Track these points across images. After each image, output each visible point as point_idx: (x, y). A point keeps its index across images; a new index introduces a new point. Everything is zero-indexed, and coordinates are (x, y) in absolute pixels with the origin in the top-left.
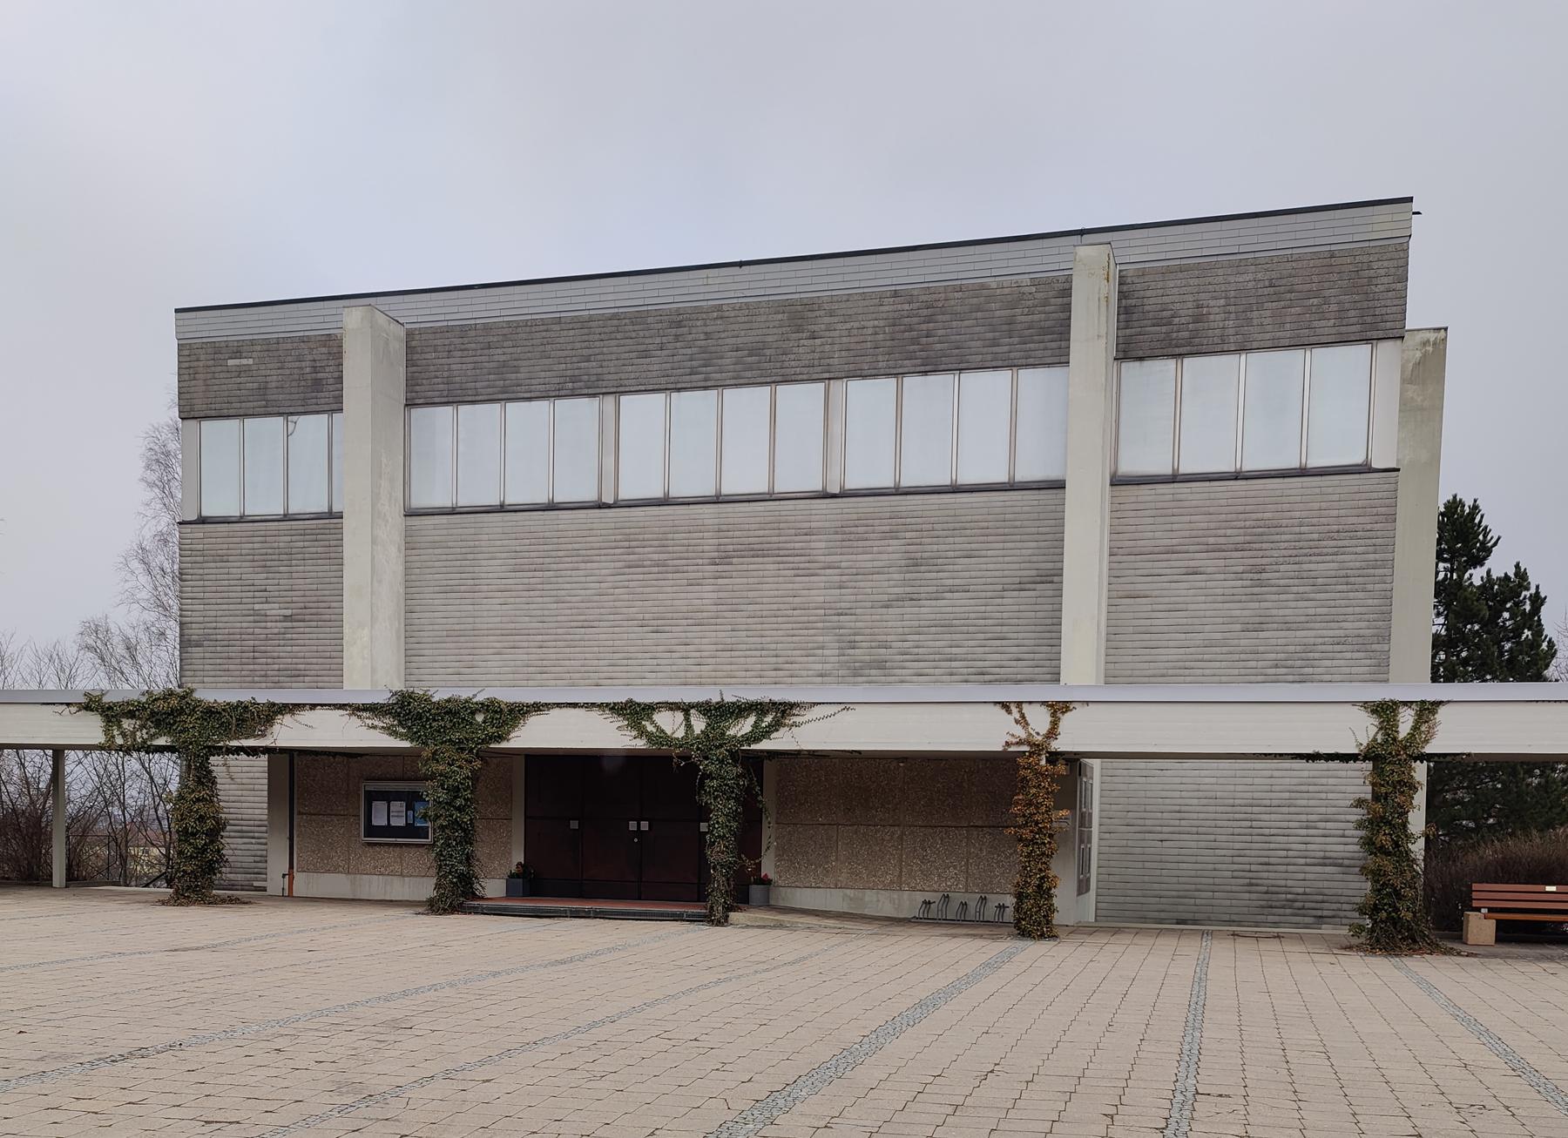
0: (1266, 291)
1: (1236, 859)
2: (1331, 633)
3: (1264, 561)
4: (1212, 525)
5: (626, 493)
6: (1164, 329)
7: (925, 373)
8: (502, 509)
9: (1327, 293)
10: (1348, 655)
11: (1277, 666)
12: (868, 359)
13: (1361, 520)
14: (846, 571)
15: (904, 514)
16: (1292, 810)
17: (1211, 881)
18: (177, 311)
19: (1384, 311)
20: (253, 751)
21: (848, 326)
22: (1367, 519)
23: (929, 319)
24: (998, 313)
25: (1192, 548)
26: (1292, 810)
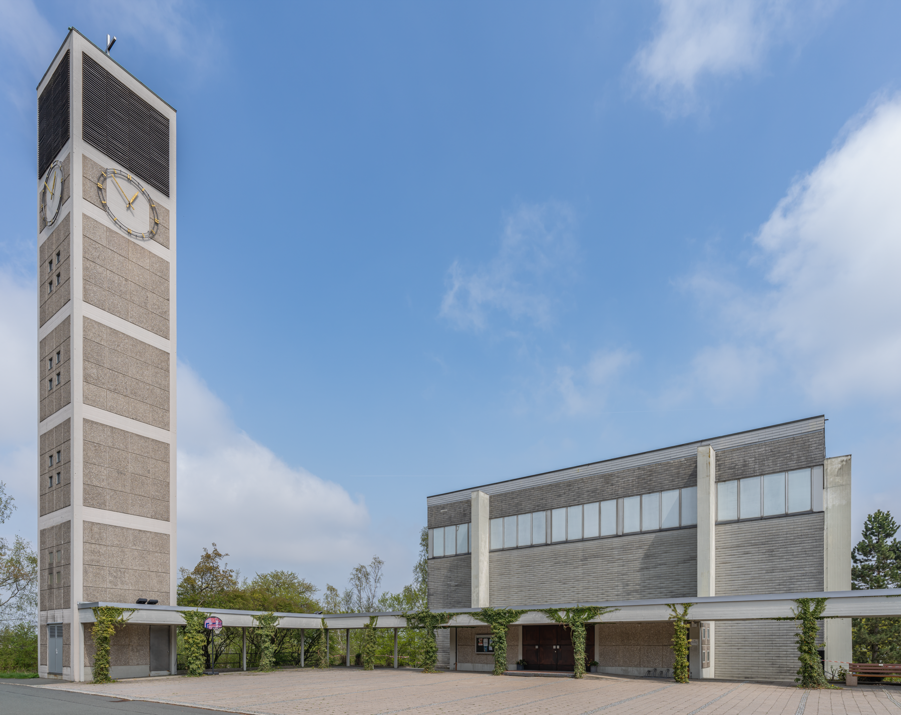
0: (770, 454)
1: (767, 655)
2: (800, 572)
3: (773, 548)
4: (753, 536)
5: (554, 540)
6: (732, 470)
7: (650, 493)
8: (517, 548)
9: (793, 452)
10: (808, 580)
11: (780, 585)
12: (630, 490)
13: (810, 531)
14: (625, 561)
15: (643, 540)
16: (788, 637)
17: (757, 663)
18: (428, 497)
19: (815, 456)
20: (444, 627)
21: (624, 480)
22: (813, 530)
23: (650, 475)
24: (674, 471)
25: (746, 545)
26: (788, 637)
